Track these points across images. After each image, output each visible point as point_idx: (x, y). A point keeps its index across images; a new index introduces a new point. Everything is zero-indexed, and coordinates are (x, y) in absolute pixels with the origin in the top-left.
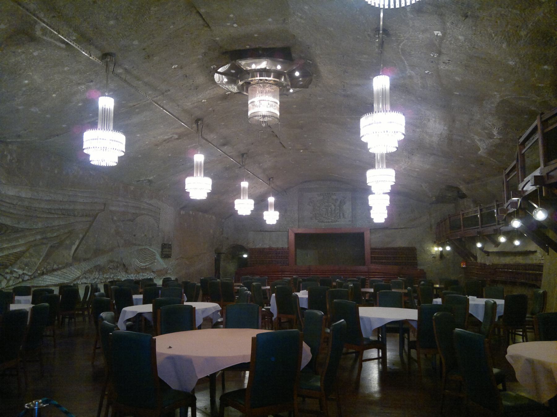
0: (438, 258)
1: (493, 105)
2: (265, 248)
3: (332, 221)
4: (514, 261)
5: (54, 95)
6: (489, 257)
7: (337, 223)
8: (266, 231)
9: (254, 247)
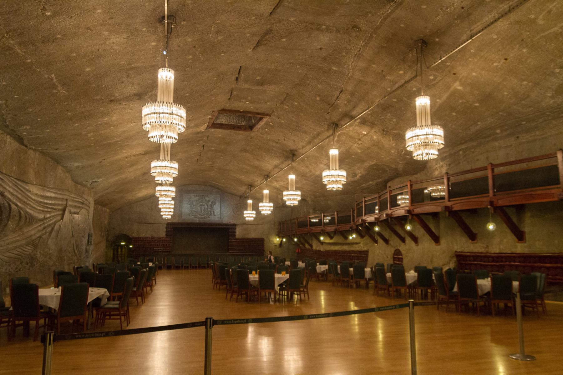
2: (147, 237)
3: (204, 217)
6: (323, 246)
7: (209, 219)
8: (150, 223)
9: (137, 236)
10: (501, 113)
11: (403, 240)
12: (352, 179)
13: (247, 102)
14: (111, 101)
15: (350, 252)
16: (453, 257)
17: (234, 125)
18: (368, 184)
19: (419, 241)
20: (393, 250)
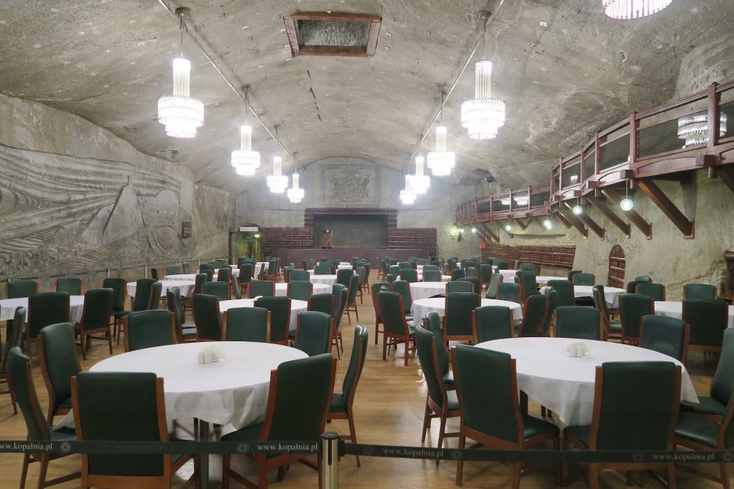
0: (456, 238)
1: (565, 97)
4: (540, 243)
5: (108, 51)
6: (513, 239)
7: (359, 203)
9: (270, 227)
11: (626, 229)
12: (545, 129)
15: (551, 249)
17: (338, 47)
18: (573, 137)
19: (653, 232)
20: (609, 247)
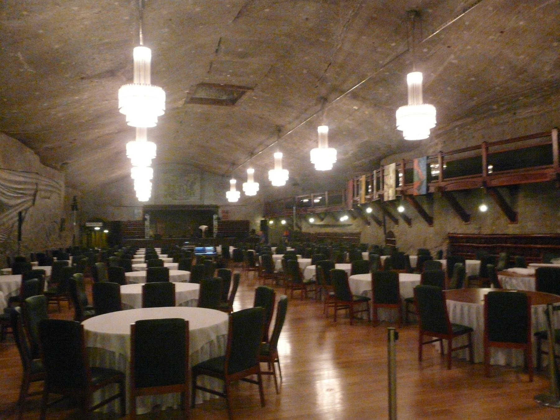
7: (189, 200)
10: (497, 88)
11: (396, 222)
13: (229, 76)
14: (82, 78)
16: (446, 239)
19: (412, 223)
